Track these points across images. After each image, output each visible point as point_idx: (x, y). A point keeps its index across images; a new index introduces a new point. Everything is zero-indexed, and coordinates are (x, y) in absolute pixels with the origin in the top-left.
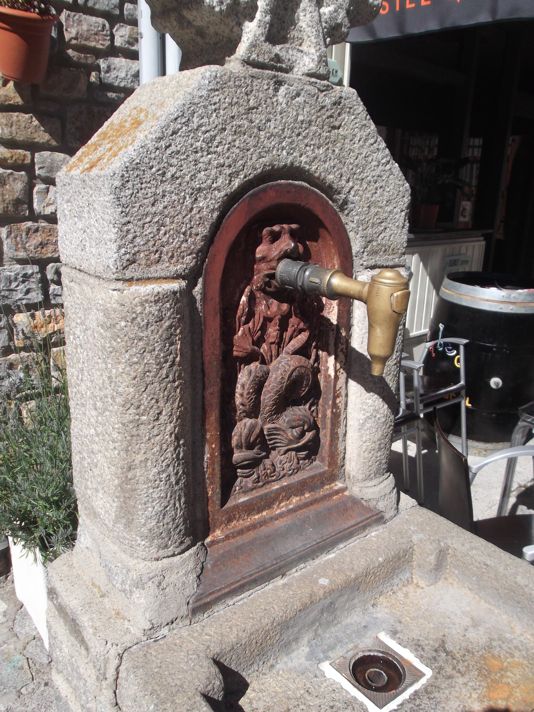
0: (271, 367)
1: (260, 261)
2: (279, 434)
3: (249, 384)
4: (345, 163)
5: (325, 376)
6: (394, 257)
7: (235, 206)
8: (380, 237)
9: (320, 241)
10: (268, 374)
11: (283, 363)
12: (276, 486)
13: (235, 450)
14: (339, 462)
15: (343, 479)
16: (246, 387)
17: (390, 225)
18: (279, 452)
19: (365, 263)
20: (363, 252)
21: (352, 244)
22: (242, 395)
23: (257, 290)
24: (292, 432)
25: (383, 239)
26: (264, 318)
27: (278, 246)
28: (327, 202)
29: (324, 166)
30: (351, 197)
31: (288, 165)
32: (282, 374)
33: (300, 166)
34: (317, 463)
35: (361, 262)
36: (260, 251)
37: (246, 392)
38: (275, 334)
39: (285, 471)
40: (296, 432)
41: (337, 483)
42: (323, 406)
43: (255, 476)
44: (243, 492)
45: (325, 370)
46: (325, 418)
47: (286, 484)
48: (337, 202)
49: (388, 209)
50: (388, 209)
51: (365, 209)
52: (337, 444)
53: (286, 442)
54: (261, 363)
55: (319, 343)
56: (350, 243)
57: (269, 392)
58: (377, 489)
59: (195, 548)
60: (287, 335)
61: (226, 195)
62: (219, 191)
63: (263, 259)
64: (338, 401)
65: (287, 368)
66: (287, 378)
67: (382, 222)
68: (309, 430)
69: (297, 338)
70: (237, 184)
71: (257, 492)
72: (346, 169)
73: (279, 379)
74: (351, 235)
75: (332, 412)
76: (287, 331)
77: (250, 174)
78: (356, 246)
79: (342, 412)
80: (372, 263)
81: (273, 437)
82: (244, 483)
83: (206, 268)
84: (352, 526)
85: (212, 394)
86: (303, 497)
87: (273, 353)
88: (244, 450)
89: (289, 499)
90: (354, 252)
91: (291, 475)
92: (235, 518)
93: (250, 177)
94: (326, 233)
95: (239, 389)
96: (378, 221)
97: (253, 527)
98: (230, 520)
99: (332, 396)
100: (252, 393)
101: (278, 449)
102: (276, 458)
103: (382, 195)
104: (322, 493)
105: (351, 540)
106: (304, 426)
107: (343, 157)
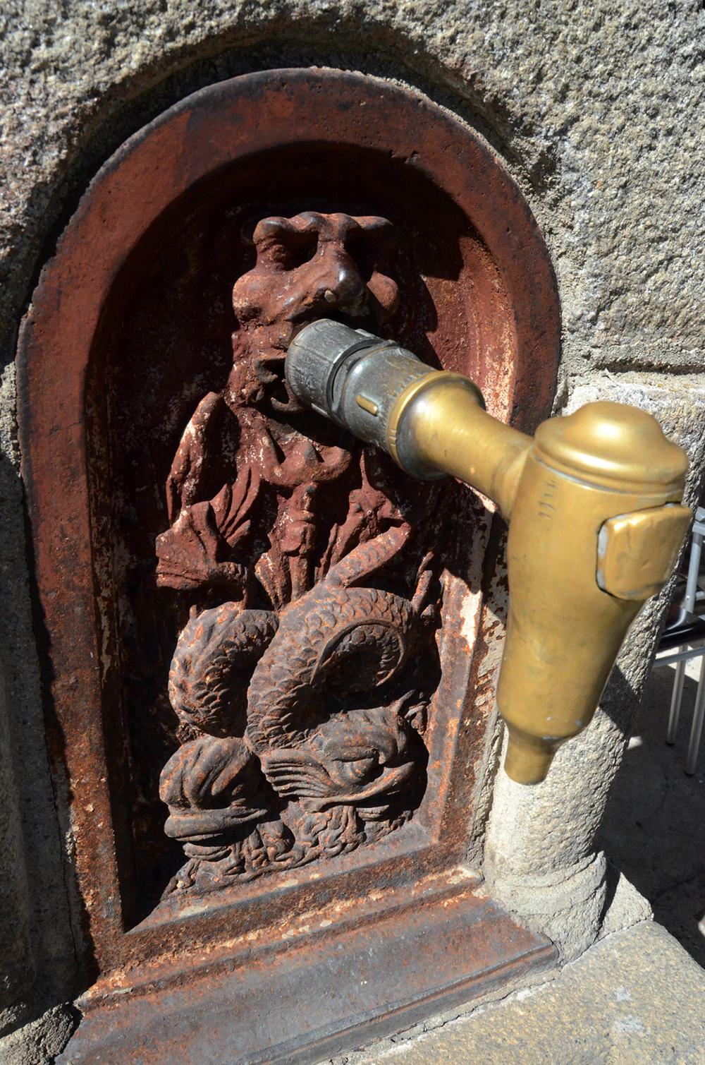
0: (284, 614)
1: (246, 319)
2: (300, 781)
3: (204, 665)
4: (556, 35)
5: (452, 641)
6: (687, 342)
7: (136, 135)
8: (650, 283)
9: (463, 276)
10: (271, 633)
11: (317, 611)
12: (289, 882)
13: (170, 807)
14: (470, 828)
15: (477, 861)
16: (195, 668)
17: (686, 252)
18: (306, 806)
19: (596, 353)
20: (594, 321)
21: (562, 293)
22: (182, 687)
23: (243, 405)
24: (340, 769)
25: (658, 289)
26: (264, 485)
27: (303, 277)
28: (488, 156)
29: (478, 33)
30: (567, 149)
31: (344, 12)
32: (307, 641)
33: (388, 23)
34: (414, 824)
35: (586, 348)
36: (244, 289)
37: (192, 682)
38: (299, 530)
39: (320, 848)
40: (352, 770)
41: (460, 868)
42: (441, 709)
43: (231, 860)
44: (195, 893)
45: (452, 625)
46: (443, 735)
47: (316, 876)
48: (522, 162)
49: (688, 201)
50: (688, 201)
51: (610, 192)
52: (469, 792)
53: (326, 789)
54: (248, 606)
55: (444, 556)
56: (556, 289)
57: (268, 681)
58: (553, 895)
59: (35, 1024)
60: (340, 534)
61: (93, 92)
62: (64, 74)
63: (254, 313)
64: (480, 701)
65: (328, 623)
66: (321, 653)
67: (661, 239)
68: (392, 763)
69: (372, 542)
70: (136, 57)
72: (556, 56)
73: (297, 654)
74: (563, 267)
76: (342, 521)
77: (192, 26)
78: (574, 303)
79: (490, 725)
80: (616, 353)
81: (287, 777)
82: (200, 872)
83: (27, 334)
84: (471, 979)
85: (72, 688)
86: (363, 901)
87: (294, 580)
88: (194, 808)
89: (324, 905)
90: (566, 316)
91: (338, 854)
93: (190, 39)
94: (479, 251)
95: (175, 673)
96: (651, 234)
97: (217, 968)
98: (151, 952)
99: (463, 689)
100: (211, 686)
101: (302, 802)
102: (296, 817)
103: (669, 157)
104: (415, 891)
105: (463, 1008)
106: (376, 757)
107: (552, 15)
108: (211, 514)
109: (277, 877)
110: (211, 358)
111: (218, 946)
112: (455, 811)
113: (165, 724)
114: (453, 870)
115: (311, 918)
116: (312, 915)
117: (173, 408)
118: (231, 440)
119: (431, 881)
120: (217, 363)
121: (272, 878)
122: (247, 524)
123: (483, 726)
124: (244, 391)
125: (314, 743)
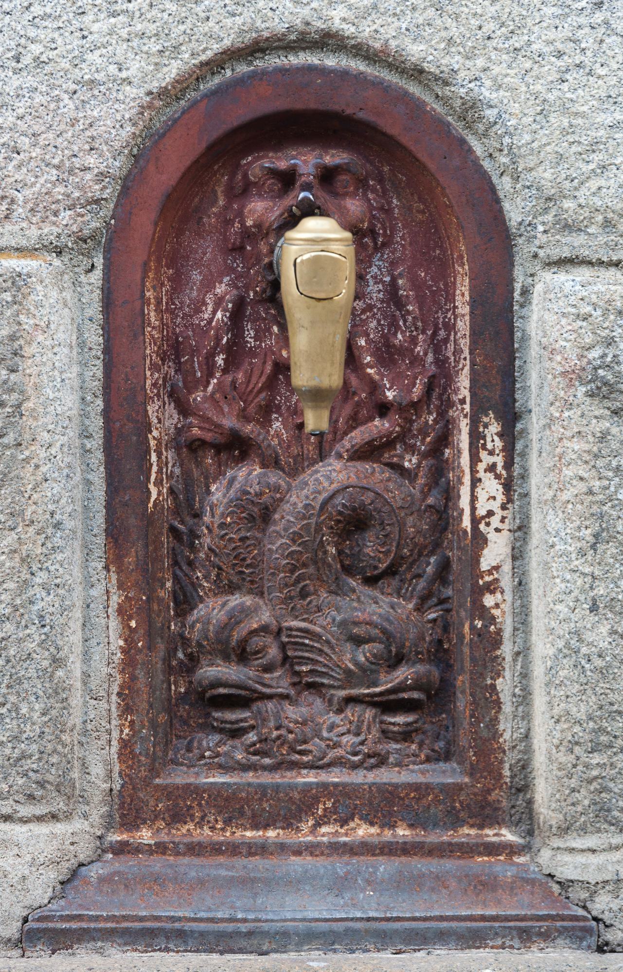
12: (310, 778)
71: (258, 777)
75: (473, 627)
92: (192, 817)
108: (234, 382)
109: (300, 773)
110: (235, 265)
111: (239, 834)
112: (485, 741)
113: (200, 572)
114: (495, 831)
115: (332, 833)
116: (333, 831)
117: (209, 301)
118: (252, 329)
119: (468, 835)
120: (239, 269)
121: (294, 773)
122: (263, 395)
123: (499, 632)
124: (258, 289)
125: (328, 619)
